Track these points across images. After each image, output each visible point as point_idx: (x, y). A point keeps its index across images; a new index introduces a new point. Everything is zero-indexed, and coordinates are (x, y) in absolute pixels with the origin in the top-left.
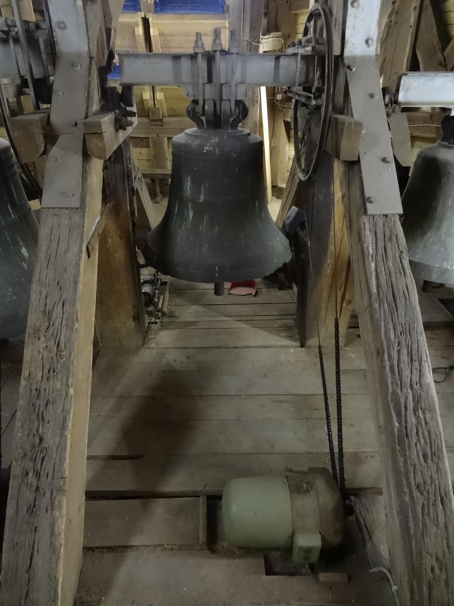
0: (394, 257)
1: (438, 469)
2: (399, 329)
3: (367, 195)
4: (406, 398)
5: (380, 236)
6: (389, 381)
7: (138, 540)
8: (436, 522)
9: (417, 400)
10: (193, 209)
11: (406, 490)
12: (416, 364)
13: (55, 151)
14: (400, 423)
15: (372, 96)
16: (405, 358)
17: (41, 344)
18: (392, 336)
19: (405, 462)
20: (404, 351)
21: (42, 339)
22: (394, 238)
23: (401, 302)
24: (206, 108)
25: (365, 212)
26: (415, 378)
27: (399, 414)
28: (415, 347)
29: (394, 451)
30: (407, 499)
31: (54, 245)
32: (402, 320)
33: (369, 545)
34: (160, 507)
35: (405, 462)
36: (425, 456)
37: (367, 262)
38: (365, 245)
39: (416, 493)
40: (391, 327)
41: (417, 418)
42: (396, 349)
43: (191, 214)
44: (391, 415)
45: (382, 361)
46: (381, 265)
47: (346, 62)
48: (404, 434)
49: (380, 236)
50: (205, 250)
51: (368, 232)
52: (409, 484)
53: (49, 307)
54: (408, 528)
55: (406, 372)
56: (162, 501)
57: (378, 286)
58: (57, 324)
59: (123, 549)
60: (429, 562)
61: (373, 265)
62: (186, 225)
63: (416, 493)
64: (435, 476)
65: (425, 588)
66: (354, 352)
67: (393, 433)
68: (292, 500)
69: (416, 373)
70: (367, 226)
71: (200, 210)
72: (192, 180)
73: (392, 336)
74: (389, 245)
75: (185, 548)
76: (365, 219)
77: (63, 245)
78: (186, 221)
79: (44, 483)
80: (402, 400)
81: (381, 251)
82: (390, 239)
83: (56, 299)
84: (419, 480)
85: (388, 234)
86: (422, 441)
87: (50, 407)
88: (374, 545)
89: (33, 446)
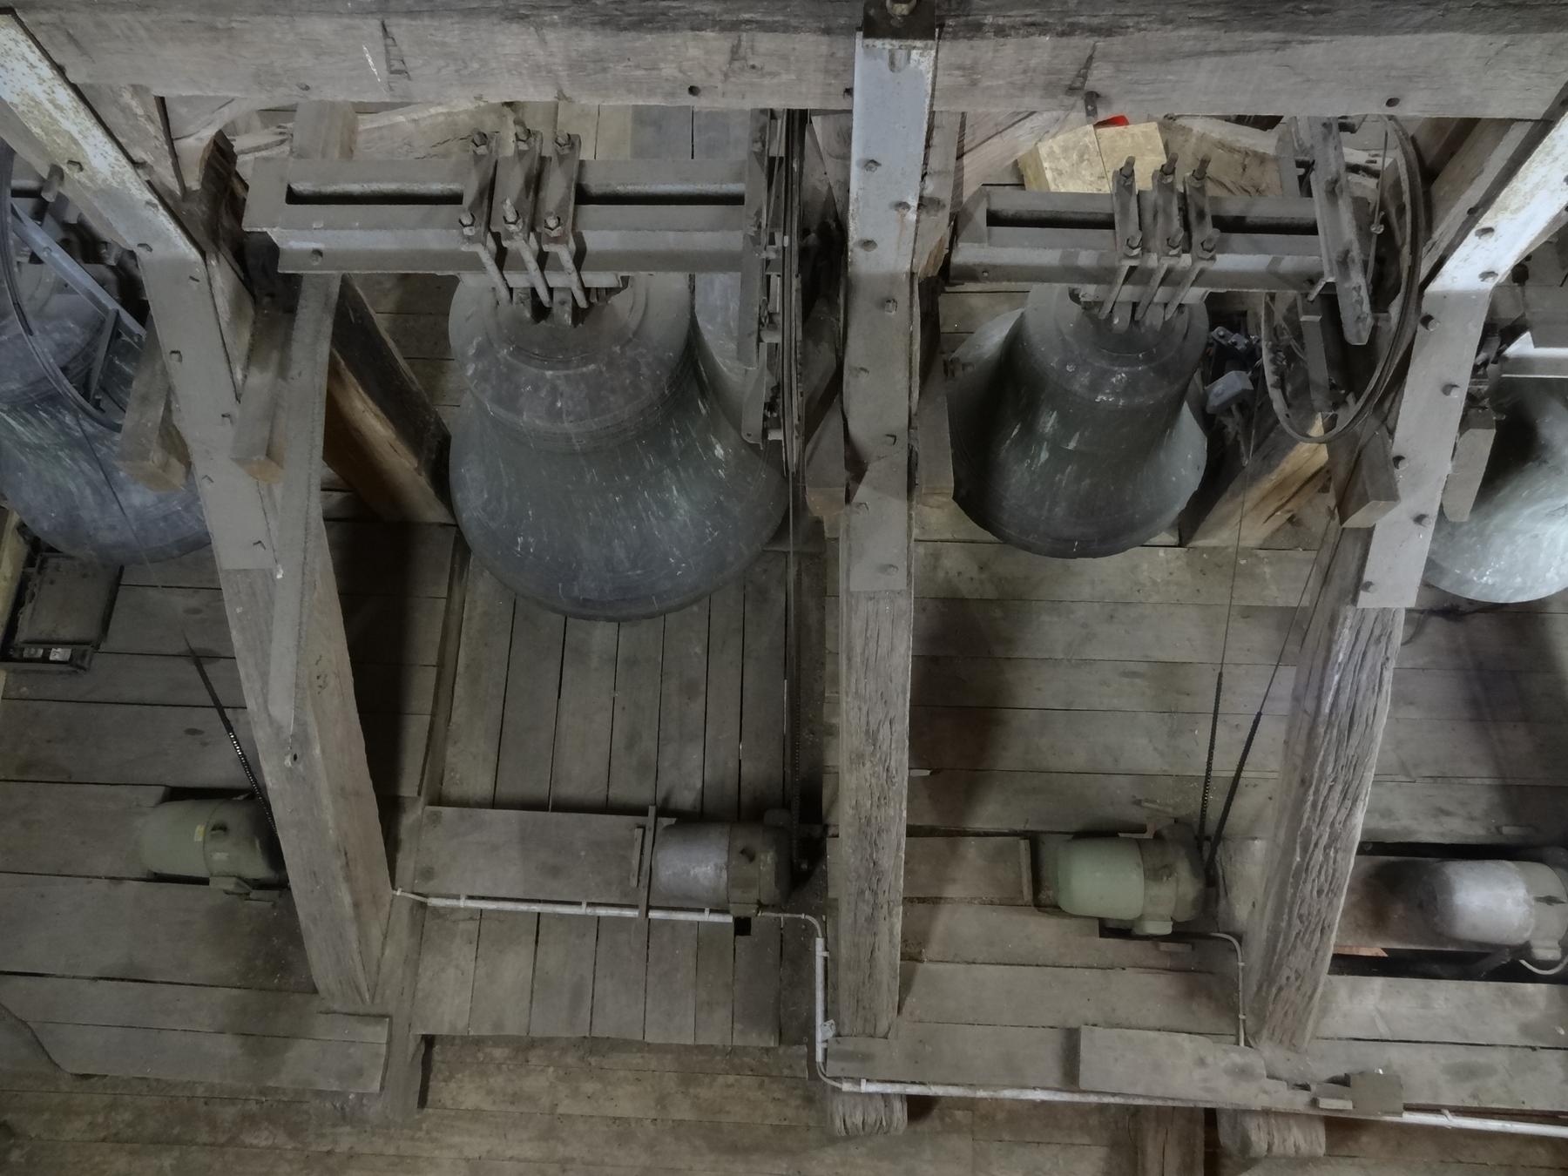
0: (1374, 666)
1: (1330, 903)
2: (1343, 761)
3: (1367, 577)
4: (1320, 837)
5: (1364, 635)
6: (1306, 816)
7: (951, 891)
8: (1308, 946)
9: (1334, 838)
10: (1051, 451)
11: (1286, 917)
12: (1348, 803)
13: (862, 492)
14: (1303, 858)
15: (1448, 388)
16: (1336, 795)
17: (867, 770)
18: (1329, 769)
19: (1294, 894)
20: (1339, 788)
21: (868, 764)
22: (1384, 640)
23: (1358, 728)
24: (1116, 321)
25: (1354, 601)
26: (1341, 817)
27: (1305, 850)
28: (1355, 783)
29: (1283, 884)
30: (1284, 924)
31: (872, 644)
32: (1351, 752)
33: (1223, 902)
34: (972, 849)
35: (1294, 894)
36: (1320, 892)
37: (1329, 672)
38: (1335, 648)
39: (1296, 922)
40: (1332, 759)
41: (1326, 855)
42: (1329, 783)
43: (1044, 455)
44: (1294, 850)
45: (1306, 793)
46: (1349, 678)
47: (1426, 307)
48: (1305, 868)
49: (1364, 635)
50: (1060, 511)
51: (1346, 631)
52: (1291, 912)
53: (873, 727)
54: (1275, 947)
55: (1332, 811)
56: (972, 841)
57: (1334, 705)
58: (884, 748)
59: (936, 901)
60: (1286, 972)
61: (1337, 678)
62: (1030, 466)
63: (1296, 922)
64: (1323, 910)
65: (1274, 990)
66: (1270, 563)
67: (1289, 866)
68: (1146, 888)
69: (1344, 812)
70: (1348, 623)
71: (1060, 456)
72: (1062, 419)
73: (1329, 769)
74: (1372, 649)
75: (1011, 903)
76: (1349, 612)
77: (885, 643)
78: (1032, 459)
79: (882, 899)
80: (1314, 839)
81: (1357, 657)
82: (1378, 640)
83: (881, 716)
84: (1304, 911)
85: (1377, 632)
86: (1323, 878)
87: (884, 835)
88: (1229, 904)
89: (868, 870)
